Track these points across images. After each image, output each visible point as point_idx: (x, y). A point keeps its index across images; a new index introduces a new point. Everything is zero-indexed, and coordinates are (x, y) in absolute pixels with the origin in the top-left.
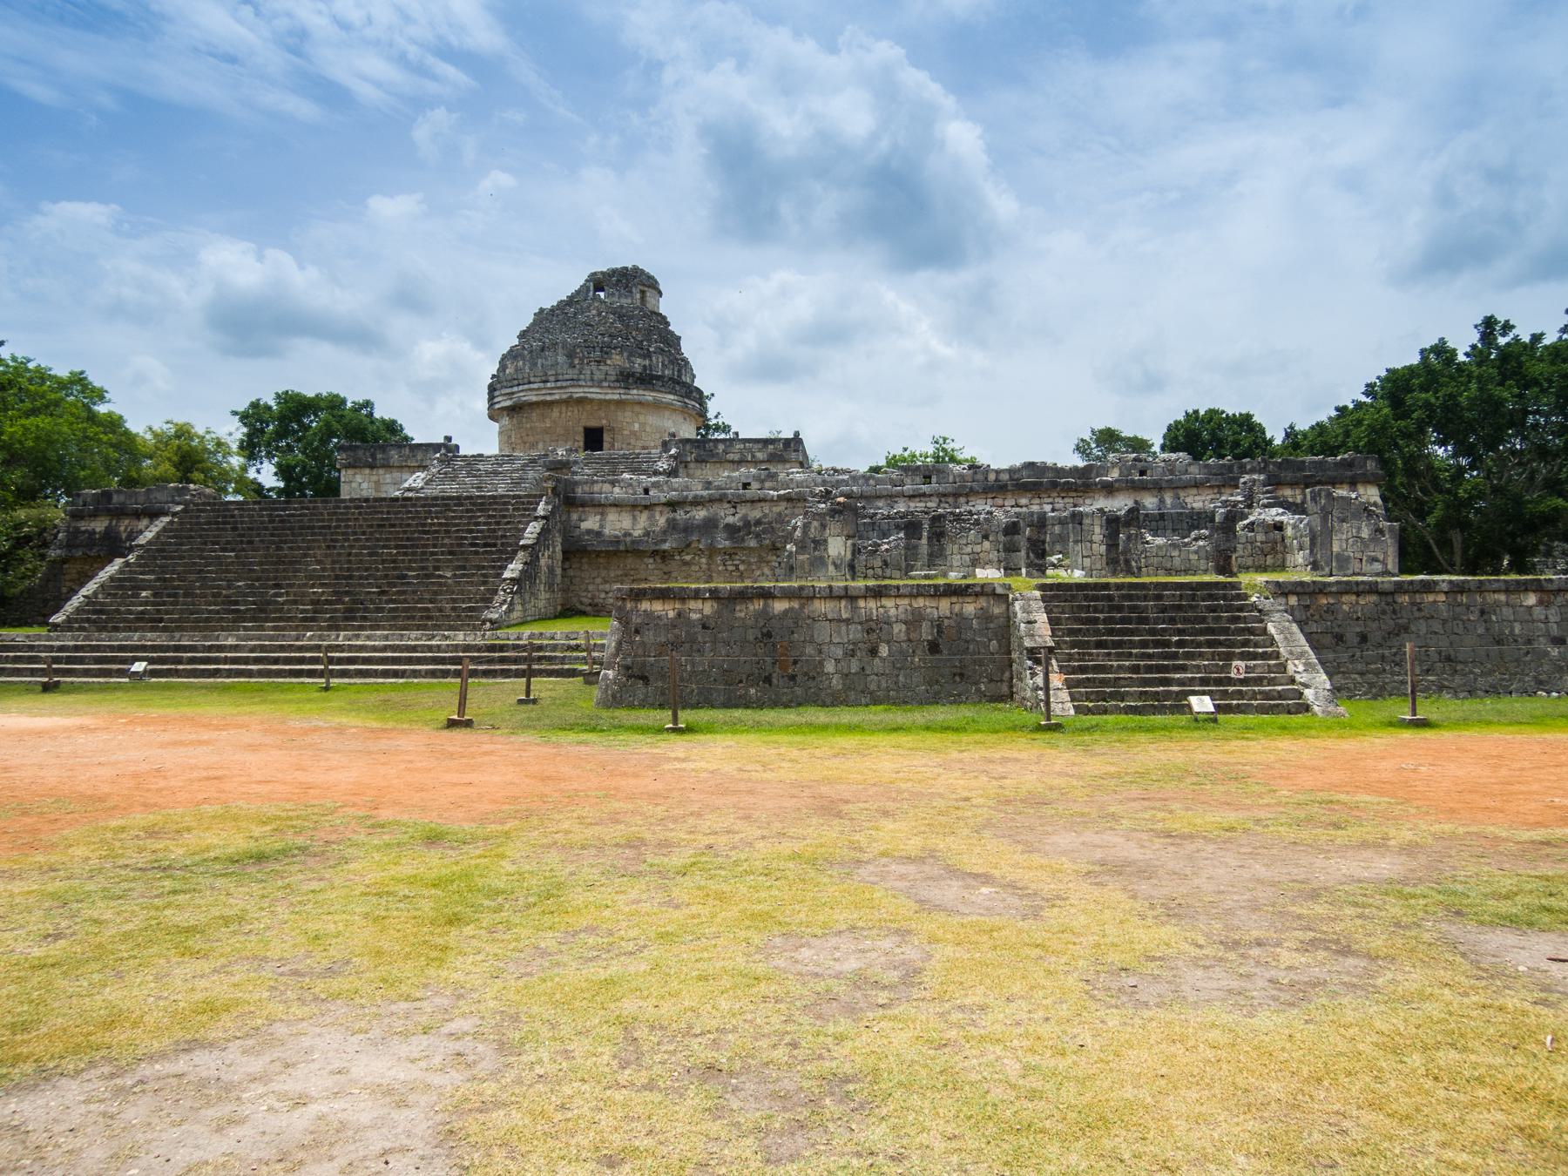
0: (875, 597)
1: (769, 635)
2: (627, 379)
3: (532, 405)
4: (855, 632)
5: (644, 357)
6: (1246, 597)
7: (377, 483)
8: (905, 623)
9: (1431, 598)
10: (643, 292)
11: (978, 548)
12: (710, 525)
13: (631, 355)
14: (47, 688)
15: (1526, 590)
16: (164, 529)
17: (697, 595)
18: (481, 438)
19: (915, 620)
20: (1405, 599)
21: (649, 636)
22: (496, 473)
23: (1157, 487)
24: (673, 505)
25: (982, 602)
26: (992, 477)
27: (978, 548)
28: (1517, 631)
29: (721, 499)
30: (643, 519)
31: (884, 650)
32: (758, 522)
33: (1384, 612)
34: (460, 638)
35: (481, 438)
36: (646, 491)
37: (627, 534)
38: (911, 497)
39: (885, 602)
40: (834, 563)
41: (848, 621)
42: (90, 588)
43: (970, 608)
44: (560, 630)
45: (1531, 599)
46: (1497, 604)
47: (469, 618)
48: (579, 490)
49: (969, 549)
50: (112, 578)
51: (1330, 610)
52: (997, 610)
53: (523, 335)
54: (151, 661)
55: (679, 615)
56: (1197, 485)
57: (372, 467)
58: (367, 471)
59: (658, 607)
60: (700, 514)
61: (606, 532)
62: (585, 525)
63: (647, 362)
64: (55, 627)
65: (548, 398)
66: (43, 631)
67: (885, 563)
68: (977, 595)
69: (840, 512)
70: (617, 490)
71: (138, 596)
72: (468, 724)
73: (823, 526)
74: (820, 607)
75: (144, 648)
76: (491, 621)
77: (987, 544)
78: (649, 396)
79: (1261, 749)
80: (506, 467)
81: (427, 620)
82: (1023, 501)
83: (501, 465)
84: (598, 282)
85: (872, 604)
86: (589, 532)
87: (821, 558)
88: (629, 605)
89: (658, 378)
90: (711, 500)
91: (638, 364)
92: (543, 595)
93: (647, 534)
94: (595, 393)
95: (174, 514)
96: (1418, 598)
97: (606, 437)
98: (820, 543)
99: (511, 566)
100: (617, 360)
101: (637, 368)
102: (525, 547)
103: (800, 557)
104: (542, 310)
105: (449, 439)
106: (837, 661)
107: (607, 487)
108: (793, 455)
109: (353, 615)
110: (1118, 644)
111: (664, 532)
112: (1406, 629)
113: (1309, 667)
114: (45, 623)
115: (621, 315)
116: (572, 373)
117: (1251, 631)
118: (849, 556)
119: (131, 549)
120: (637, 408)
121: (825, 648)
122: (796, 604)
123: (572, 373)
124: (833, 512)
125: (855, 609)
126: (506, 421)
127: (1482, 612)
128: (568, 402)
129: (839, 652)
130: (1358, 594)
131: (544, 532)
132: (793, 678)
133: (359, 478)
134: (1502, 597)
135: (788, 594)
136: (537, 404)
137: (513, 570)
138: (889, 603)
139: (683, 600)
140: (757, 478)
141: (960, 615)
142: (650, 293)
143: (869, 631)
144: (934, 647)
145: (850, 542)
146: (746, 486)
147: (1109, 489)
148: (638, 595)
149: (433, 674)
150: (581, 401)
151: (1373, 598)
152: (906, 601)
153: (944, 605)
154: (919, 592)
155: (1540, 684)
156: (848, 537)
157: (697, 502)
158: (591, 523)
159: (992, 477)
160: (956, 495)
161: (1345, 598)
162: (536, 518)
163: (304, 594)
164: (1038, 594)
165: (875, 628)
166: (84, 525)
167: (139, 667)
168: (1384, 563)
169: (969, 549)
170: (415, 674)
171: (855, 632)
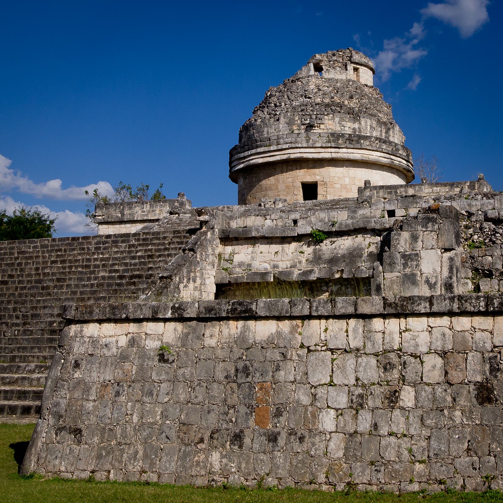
0: (397, 316)
8: (444, 354)
10: (356, 70)
13: (342, 119)
31: (408, 397)
36: (295, 222)
39: (414, 323)
40: (427, 281)
55: (133, 342)
60: (345, 244)
63: (356, 126)
69: (434, 221)
70: (268, 222)
73: (414, 238)
85: (393, 324)
87: (414, 275)
89: (366, 138)
91: (349, 127)
98: (411, 258)
103: (387, 275)
106: (340, 412)
118: (446, 273)
121: (321, 392)
122: (285, 326)
125: (368, 335)
129: (342, 401)
138: (417, 324)
143: (387, 367)
145: (447, 255)
146: (391, 213)
152: (445, 321)
156: (447, 250)
171: (370, 370)
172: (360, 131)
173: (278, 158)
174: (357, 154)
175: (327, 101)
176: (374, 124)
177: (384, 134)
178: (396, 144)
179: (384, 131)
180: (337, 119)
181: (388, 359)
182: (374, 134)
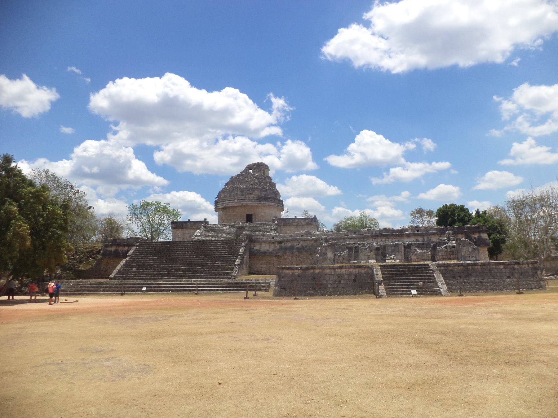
1: (315, 278)
2: (260, 199)
3: (230, 207)
4: (335, 278)
5: (265, 191)
6: (430, 267)
7: (184, 233)
9: (476, 267)
11: (369, 254)
12: (292, 248)
13: (261, 191)
14: (122, 294)
16: (135, 250)
17: (297, 268)
18: (213, 219)
19: (350, 274)
20: (470, 267)
21: (286, 279)
22: (221, 230)
23: (422, 235)
24: (280, 242)
25: (366, 270)
26: (374, 233)
27: (369, 254)
29: (295, 240)
30: (272, 246)
31: (342, 282)
32: (306, 246)
34: (226, 280)
35: (213, 219)
36: (273, 238)
37: (268, 250)
38: (351, 239)
41: (333, 275)
42: (118, 268)
43: (363, 271)
44: (253, 277)
45: (502, 267)
46: (493, 268)
47: (227, 276)
48: (254, 238)
49: (367, 254)
50: (124, 265)
51: (452, 270)
52: (370, 271)
53: (226, 185)
54: (147, 287)
56: (434, 234)
57: (182, 228)
58: (180, 230)
59: (287, 272)
61: (262, 250)
62: (255, 248)
64: (111, 279)
66: (108, 280)
67: (343, 259)
68: (365, 268)
69: (330, 246)
71: (132, 269)
72: (249, 298)
73: (326, 250)
74: (327, 271)
75: (146, 284)
76: (234, 276)
77: (372, 253)
78: (267, 203)
79: (427, 303)
80: (224, 228)
81: (215, 276)
82: (383, 240)
83: (222, 227)
84: (249, 167)
85: (339, 270)
86: (257, 250)
88: (280, 271)
89: (270, 198)
90: (292, 240)
91: (263, 194)
92: (245, 269)
93: (274, 250)
94: (250, 203)
95: (137, 246)
96: (473, 267)
97: (253, 217)
98: (325, 254)
99: (237, 260)
100: (257, 192)
101: (263, 195)
102: (240, 255)
104: (232, 177)
105: (206, 219)
107: (262, 237)
108: (314, 223)
109: (194, 274)
110: (398, 279)
111: (279, 250)
112: (471, 275)
113: (442, 284)
114: (108, 278)
115: (257, 178)
116: (243, 197)
117: (430, 276)
119: (127, 256)
122: (321, 271)
123: (243, 197)
124: (328, 246)
125: (335, 271)
126: (221, 212)
127: (489, 270)
130: (458, 266)
131: (245, 251)
132: (320, 288)
133: (178, 232)
134: (494, 267)
135: (319, 268)
136: (231, 207)
137: (238, 261)
138: (343, 270)
139: (293, 270)
140: (305, 234)
141: (361, 273)
142: (266, 170)
143: (339, 277)
144: (355, 280)
147: (408, 236)
148: (283, 269)
149: (222, 290)
150: (245, 206)
151: (462, 267)
152: (347, 270)
153: (357, 270)
154: (351, 267)
155: (504, 288)
157: (288, 241)
158: (257, 247)
159: (374, 233)
160: (364, 238)
161: (455, 267)
162: (242, 247)
163: (179, 269)
164: (379, 267)
165: (340, 276)
166: (108, 249)
167: (144, 289)
168: (476, 257)
169: (367, 254)
170: (217, 290)
171: (335, 278)
181: (339, 276)
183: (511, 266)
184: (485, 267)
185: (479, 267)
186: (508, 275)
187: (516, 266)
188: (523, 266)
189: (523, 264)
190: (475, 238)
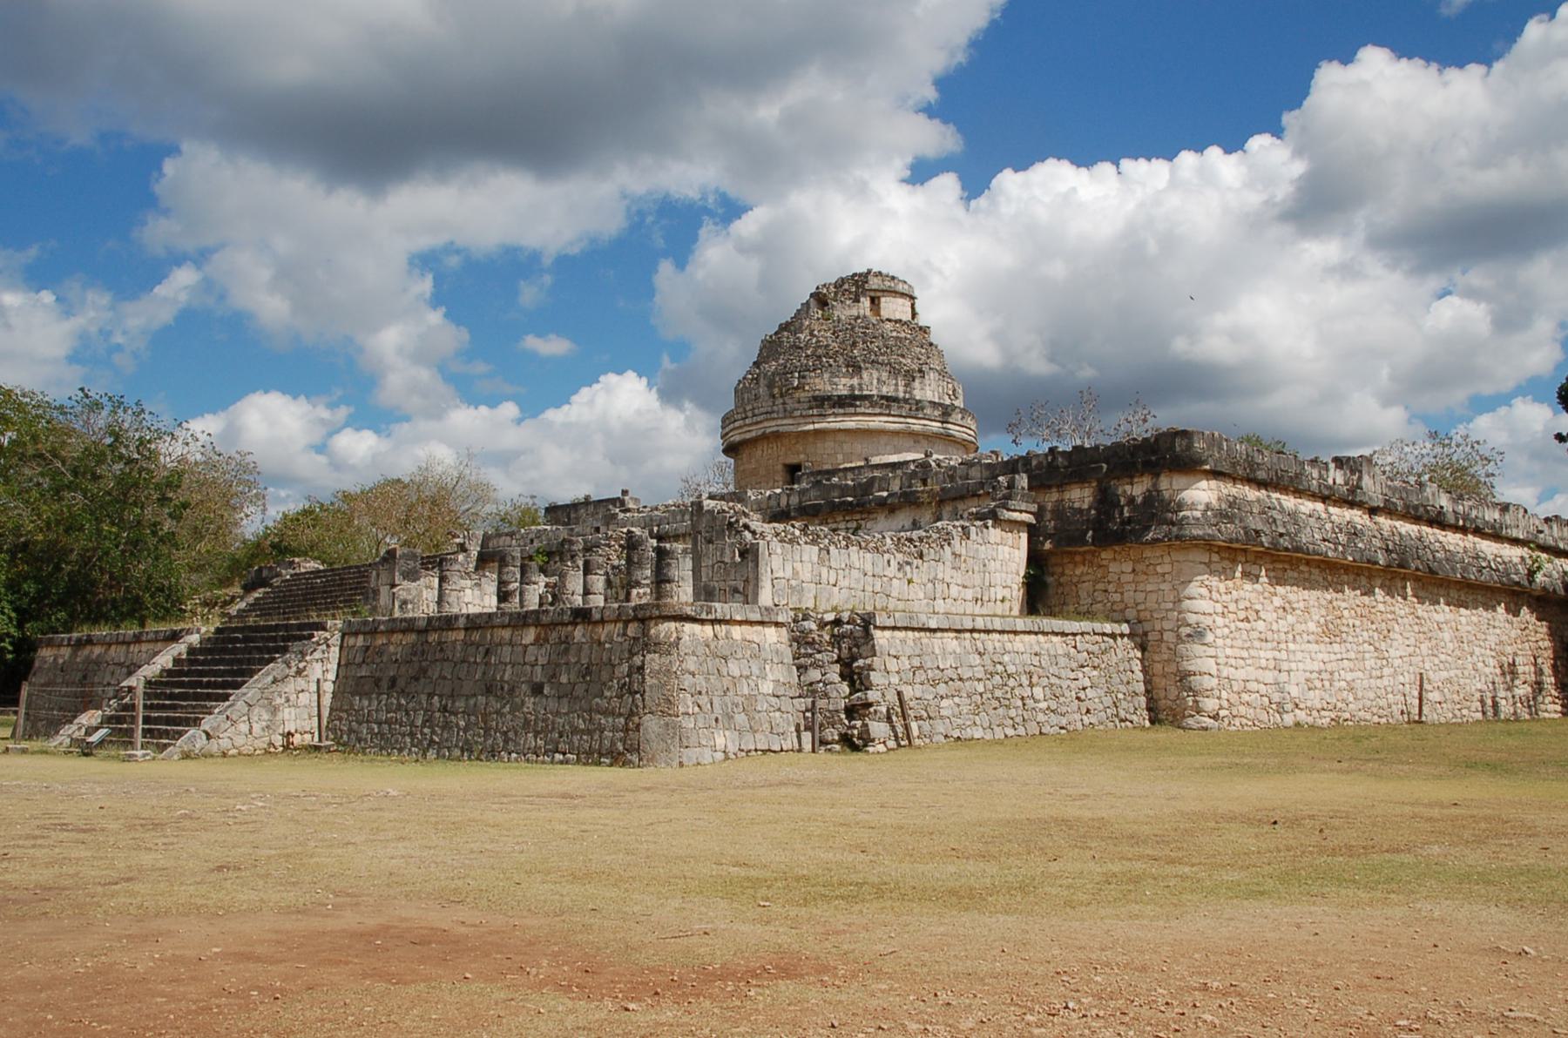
15: (526, 625)
28: (506, 678)
33: (415, 654)
41: (121, 665)
45: (530, 635)
51: (380, 653)
63: (855, 381)
65: (748, 436)
91: (843, 385)
120: (841, 437)
127: (487, 652)
128: (765, 437)
130: (404, 631)
134: (506, 634)
150: (777, 436)
151: (412, 638)
172: (861, 389)
173: (754, 434)
174: (850, 423)
175: (820, 351)
176: (885, 375)
177: (901, 389)
178: (918, 402)
179: (901, 383)
180: (826, 376)
182: (885, 390)
183: (564, 631)
184: (476, 636)
185: (461, 635)
186: (539, 675)
187: (579, 633)
188: (603, 632)
189: (602, 621)
190: (1131, 500)
